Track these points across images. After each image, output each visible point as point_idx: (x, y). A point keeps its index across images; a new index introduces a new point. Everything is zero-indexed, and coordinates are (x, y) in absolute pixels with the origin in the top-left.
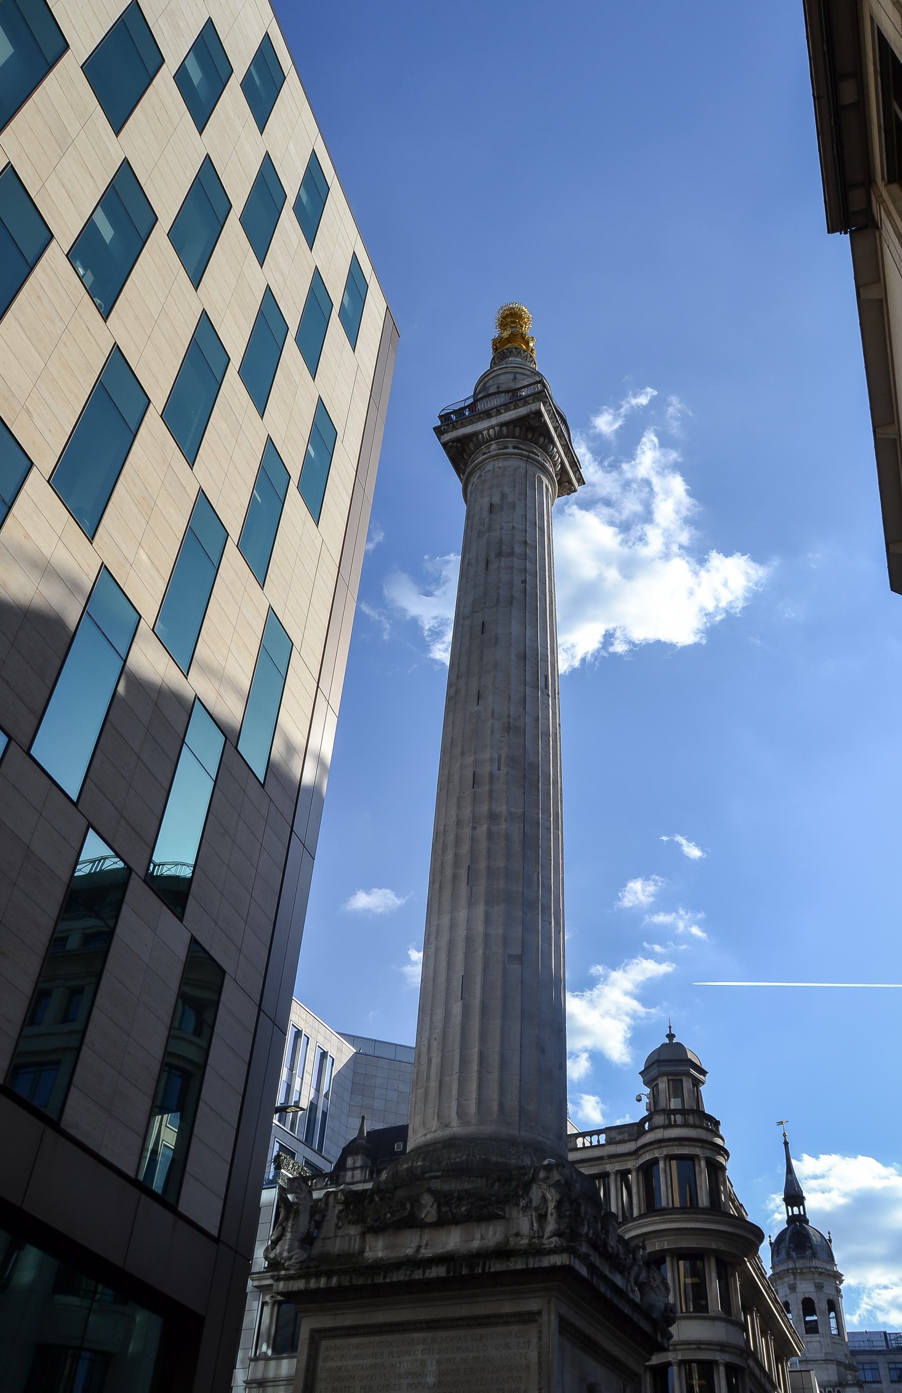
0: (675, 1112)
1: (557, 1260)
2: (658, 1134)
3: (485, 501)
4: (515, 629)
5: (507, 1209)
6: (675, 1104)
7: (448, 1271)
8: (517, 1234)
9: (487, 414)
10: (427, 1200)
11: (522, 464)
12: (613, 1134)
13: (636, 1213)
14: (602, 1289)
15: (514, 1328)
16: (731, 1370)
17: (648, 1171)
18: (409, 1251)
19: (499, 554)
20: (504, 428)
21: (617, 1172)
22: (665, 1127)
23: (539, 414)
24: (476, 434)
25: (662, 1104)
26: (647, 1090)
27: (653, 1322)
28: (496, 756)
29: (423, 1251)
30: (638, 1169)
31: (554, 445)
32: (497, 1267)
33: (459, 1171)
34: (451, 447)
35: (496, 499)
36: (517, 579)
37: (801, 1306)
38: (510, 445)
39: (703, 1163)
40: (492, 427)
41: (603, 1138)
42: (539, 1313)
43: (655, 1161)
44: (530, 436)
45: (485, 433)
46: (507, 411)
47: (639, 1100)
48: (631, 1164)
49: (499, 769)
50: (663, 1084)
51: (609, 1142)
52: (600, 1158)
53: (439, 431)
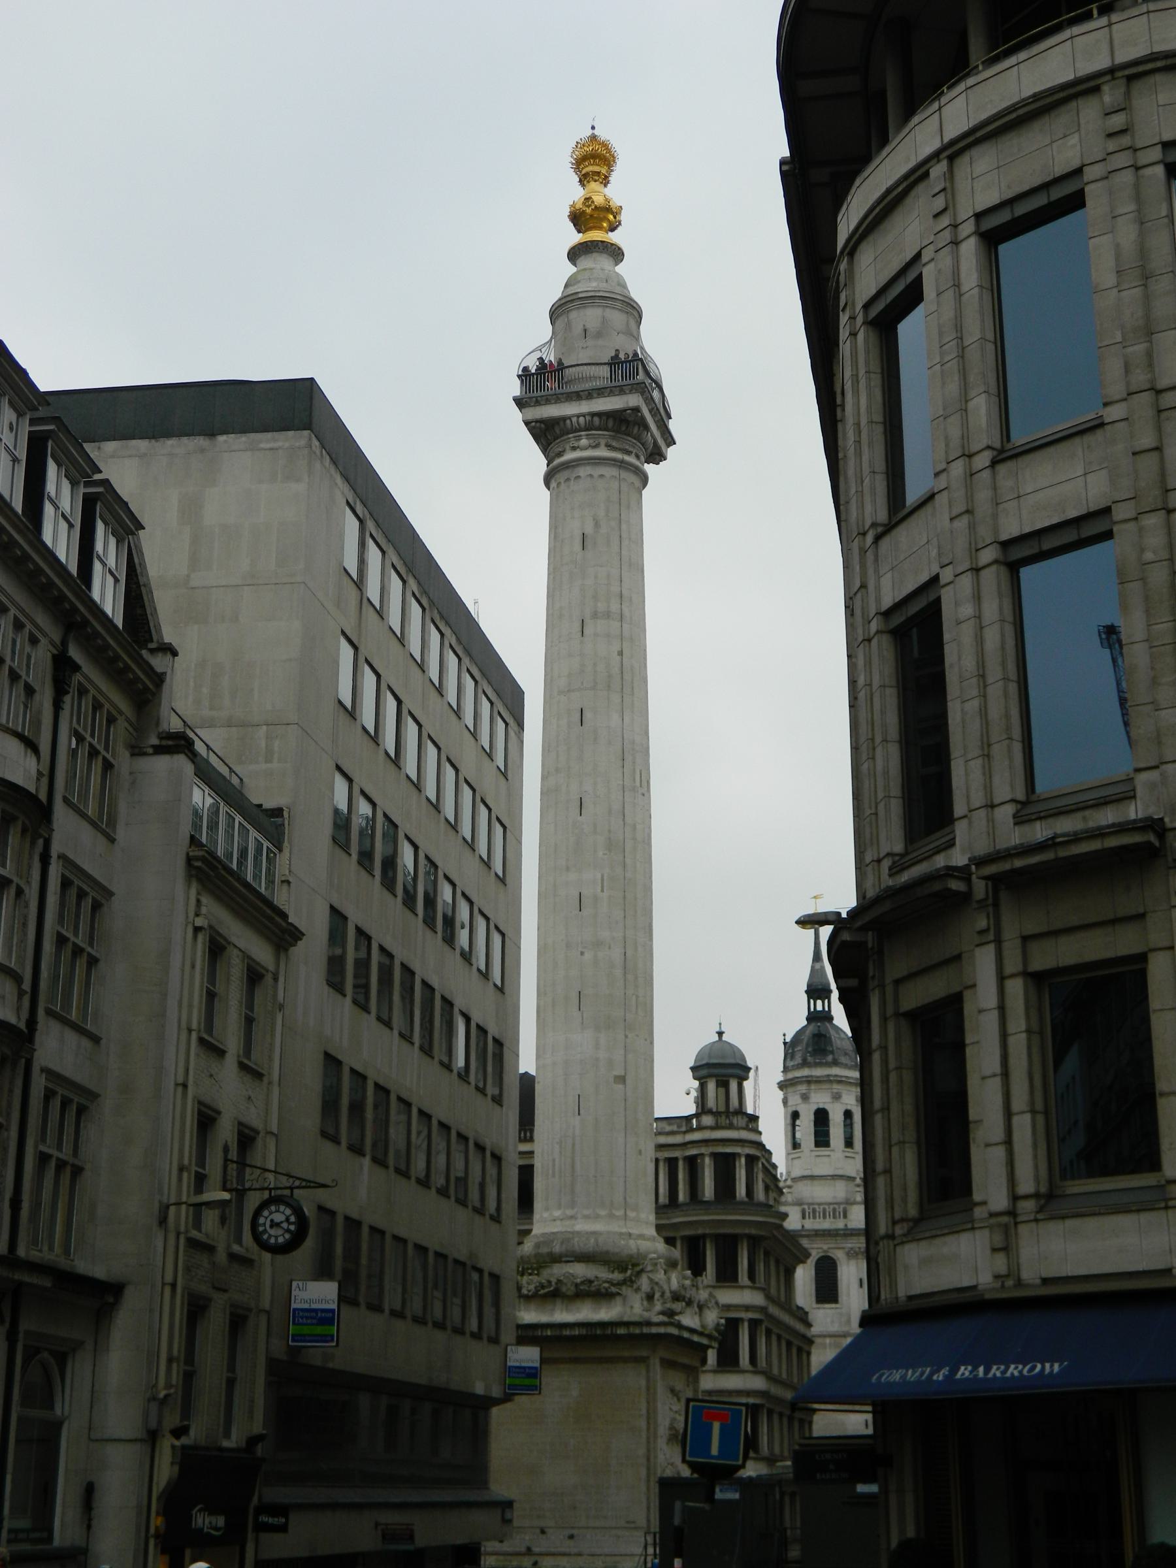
2: (707, 1135)
16: (754, 1324)
17: (693, 1163)
19: (595, 615)
20: (596, 419)
22: (712, 1128)
24: (564, 419)
25: (711, 1103)
26: (696, 1084)
28: (599, 876)
32: (621, 1331)
34: (534, 427)
35: (589, 530)
36: (616, 648)
37: (812, 1117)
38: (603, 442)
44: (624, 428)
45: (574, 419)
48: (676, 1154)
49: (602, 891)
53: (520, 403)
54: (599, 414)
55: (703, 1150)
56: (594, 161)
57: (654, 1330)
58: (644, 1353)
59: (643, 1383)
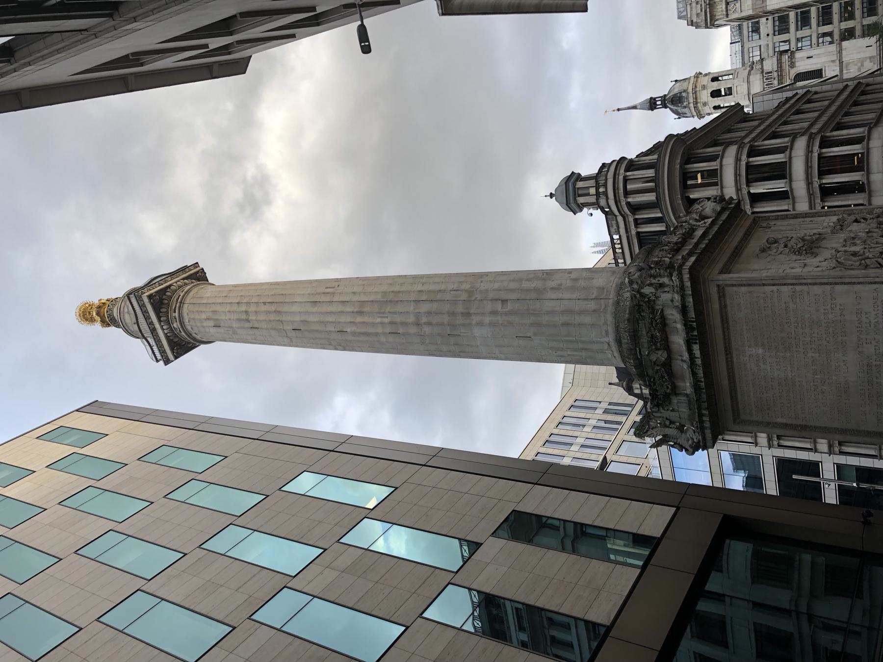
0: (597, 190)
1: (686, 277)
2: (612, 202)
3: (213, 331)
4: (296, 308)
5: (657, 307)
6: (593, 191)
7: (696, 343)
8: (672, 301)
9: (153, 331)
10: (653, 358)
11: (186, 306)
12: (613, 230)
13: (660, 215)
14: (704, 246)
15: (728, 301)
17: (635, 208)
18: (685, 366)
19: (248, 320)
21: (636, 227)
22: (607, 199)
23: (150, 297)
24: (167, 337)
25: (593, 199)
26: (585, 209)
27: (723, 210)
29: (684, 358)
30: (634, 214)
31: (171, 285)
32: (692, 314)
33: (635, 336)
35: (211, 323)
36: (263, 308)
39: (628, 174)
40: (162, 327)
41: (616, 237)
42: (718, 286)
43: (628, 204)
46: (150, 318)
47: (591, 214)
48: (631, 219)
50: (581, 200)
51: (618, 233)
52: (628, 237)
53: (167, 362)
54: (159, 318)
55: (624, 203)
56: (87, 314)
57: (688, 284)
58: (715, 289)
59: (744, 289)
